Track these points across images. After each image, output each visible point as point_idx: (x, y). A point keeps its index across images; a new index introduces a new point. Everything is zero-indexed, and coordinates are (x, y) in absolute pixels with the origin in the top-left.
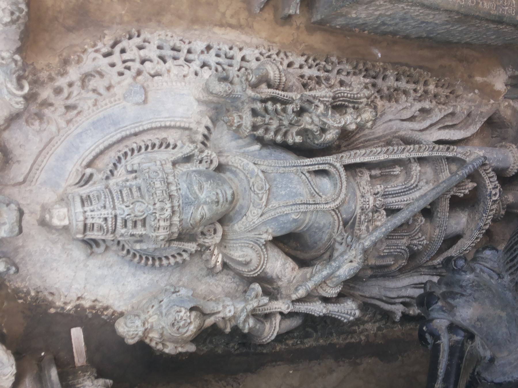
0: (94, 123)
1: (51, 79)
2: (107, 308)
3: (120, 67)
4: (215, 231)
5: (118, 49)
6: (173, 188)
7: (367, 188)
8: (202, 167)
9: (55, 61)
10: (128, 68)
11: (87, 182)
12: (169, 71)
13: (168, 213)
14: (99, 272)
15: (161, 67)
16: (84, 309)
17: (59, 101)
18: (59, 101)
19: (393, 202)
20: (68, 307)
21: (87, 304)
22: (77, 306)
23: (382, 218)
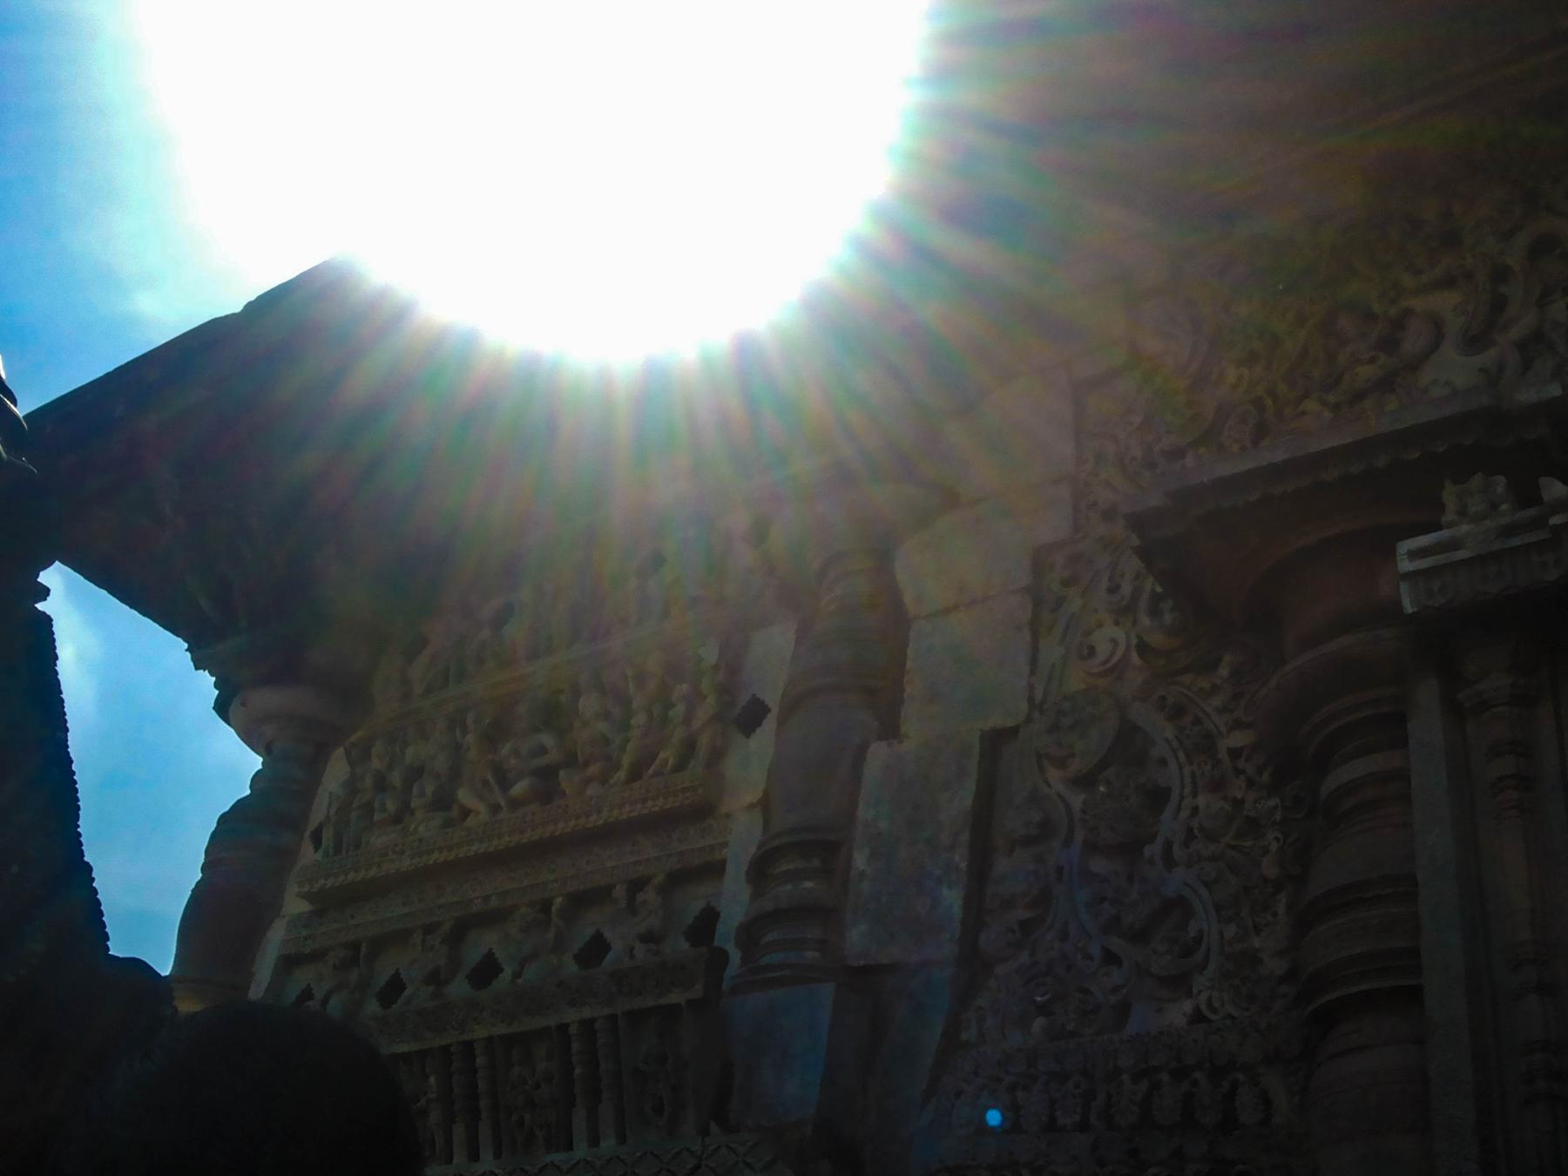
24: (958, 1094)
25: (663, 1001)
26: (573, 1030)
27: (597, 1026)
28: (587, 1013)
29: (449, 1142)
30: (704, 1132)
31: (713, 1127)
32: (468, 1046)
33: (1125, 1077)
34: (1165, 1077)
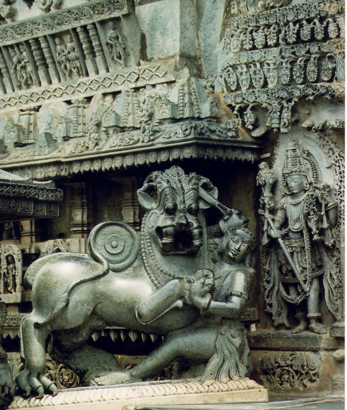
1: (331, 140)
3: (336, 159)
5: (341, 158)
6: (294, 173)
9: (335, 140)
10: (336, 162)
12: (337, 175)
13: (288, 172)
15: (338, 173)
17: (325, 142)
18: (325, 142)
19: (295, 254)
21: (275, 157)
24: (232, 36)
25: (112, 16)
26: (78, 30)
27: (88, 28)
28: (83, 23)
29: (38, 77)
30: (139, 64)
31: (142, 62)
32: (37, 40)
33: (291, 24)
34: (304, 22)
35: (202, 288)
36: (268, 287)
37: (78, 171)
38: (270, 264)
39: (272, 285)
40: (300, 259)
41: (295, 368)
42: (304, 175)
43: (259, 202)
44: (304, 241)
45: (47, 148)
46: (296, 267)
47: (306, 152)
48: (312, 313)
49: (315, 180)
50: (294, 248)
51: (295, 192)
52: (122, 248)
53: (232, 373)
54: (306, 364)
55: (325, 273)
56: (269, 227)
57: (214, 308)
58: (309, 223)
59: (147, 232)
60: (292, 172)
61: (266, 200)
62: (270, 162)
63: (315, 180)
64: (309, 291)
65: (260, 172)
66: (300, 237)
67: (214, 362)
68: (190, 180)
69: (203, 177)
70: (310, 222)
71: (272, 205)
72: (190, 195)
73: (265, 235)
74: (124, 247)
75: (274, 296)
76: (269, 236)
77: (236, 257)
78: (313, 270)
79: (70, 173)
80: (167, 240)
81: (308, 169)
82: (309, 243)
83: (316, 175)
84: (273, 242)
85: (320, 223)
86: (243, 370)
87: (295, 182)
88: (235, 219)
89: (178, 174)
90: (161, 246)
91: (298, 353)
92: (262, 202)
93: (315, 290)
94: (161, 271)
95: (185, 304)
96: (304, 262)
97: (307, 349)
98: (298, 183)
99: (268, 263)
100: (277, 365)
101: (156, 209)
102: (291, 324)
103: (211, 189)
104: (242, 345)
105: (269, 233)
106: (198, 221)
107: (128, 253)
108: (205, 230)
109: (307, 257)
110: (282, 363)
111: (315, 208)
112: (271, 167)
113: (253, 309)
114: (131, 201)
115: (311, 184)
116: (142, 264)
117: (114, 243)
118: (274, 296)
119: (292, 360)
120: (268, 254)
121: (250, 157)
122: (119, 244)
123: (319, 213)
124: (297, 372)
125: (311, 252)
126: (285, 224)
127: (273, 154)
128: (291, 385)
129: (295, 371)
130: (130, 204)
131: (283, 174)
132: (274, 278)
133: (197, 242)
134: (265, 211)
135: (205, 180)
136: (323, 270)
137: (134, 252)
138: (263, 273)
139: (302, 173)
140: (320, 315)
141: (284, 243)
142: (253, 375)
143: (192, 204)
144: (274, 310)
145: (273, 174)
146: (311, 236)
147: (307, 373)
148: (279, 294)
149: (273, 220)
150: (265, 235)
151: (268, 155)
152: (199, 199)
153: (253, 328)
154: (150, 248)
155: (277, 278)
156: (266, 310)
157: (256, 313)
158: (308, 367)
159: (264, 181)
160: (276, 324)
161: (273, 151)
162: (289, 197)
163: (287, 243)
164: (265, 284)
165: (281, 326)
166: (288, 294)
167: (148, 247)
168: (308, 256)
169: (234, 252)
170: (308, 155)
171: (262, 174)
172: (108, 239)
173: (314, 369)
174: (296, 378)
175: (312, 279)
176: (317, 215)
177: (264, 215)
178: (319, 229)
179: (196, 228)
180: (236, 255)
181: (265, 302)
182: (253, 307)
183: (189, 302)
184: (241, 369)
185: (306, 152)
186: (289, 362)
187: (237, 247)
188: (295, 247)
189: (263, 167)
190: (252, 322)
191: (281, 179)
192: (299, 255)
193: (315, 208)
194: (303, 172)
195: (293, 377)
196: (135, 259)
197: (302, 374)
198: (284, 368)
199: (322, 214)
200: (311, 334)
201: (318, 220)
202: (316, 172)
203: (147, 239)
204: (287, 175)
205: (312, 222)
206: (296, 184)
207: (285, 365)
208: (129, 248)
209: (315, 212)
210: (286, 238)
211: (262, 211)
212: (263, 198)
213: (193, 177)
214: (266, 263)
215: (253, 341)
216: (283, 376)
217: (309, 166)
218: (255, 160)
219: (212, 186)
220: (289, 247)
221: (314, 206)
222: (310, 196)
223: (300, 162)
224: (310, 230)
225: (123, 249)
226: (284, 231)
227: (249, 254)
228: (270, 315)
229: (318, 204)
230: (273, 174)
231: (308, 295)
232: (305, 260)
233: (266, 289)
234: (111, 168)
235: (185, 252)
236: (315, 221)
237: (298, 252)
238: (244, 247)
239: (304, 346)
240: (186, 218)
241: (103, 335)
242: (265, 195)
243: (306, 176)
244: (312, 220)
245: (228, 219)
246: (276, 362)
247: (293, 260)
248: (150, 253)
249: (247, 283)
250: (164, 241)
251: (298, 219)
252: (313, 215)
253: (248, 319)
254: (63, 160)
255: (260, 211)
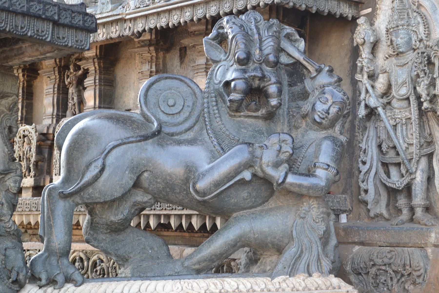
0: (434, 4)
2: (376, 19)
4: (394, 52)
6: (401, 27)
7: (404, 115)
8: (414, 42)
11: (413, 4)
13: (393, 26)
14: (387, 14)
16: (376, 11)
19: (399, 128)
20: (378, 6)
21: (378, 12)
22: (378, 9)
23: (392, 122)
35: (278, 156)
36: (364, 169)
37: (142, 29)
38: (367, 141)
39: (368, 167)
40: (405, 133)
41: (394, 268)
42: (413, 31)
43: (357, 65)
44: (410, 110)
45: (110, 4)
46: (399, 143)
47: (416, 4)
48: (418, 199)
49: (427, 37)
50: (398, 120)
51: (401, 50)
52: (181, 108)
53: (313, 268)
54: (408, 263)
55: (436, 151)
56: (368, 95)
57: (291, 184)
58: (418, 88)
59: (212, 88)
60: (398, 26)
61: (365, 62)
62: (371, 18)
63: (427, 37)
64: (416, 172)
65: (359, 28)
66: (405, 106)
67: (291, 252)
68: (271, 26)
69: (287, 27)
70: (419, 86)
71: (372, 68)
72: (269, 45)
73: (363, 104)
74: (183, 106)
75: (371, 179)
76: (367, 106)
77: (324, 121)
78: (421, 146)
79: (133, 32)
80: (235, 96)
81: (419, 23)
82: (417, 113)
83: (428, 31)
84: (372, 113)
85: (432, 88)
86: (326, 264)
87: (401, 38)
88: (324, 79)
89: (255, 19)
90: (228, 104)
91: (399, 249)
92: (359, 64)
93: (423, 171)
94: (228, 136)
95: (254, 175)
96: (410, 136)
97: (410, 245)
98: (405, 39)
99: (365, 139)
100: (372, 263)
101: (225, 60)
102: (390, 215)
103: (296, 41)
104: (327, 233)
105: (367, 102)
106: (278, 76)
107: (188, 114)
108: (286, 89)
109: (414, 130)
110: (379, 261)
111: (426, 68)
112: (372, 24)
113: (344, 196)
114: (205, 66)
115: (421, 40)
116: (204, 126)
117: (171, 102)
118: (371, 179)
119: (390, 259)
120: (365, 128)
121: (346, 10)
122: (178, 103)
123: (430, 75)
124: (396, 272)
125: (419, 124)
126: (387, 93)
127: (375, 10)
128: (388, 289)
129: (393, 271)
130: (203, 70)
131: (387, 28)
132: (372, 158)
133: (274, 102)
134: (363, 76)
135: (289, 29)
136: (433, 147)
137: (196, 113)
138: (357, 152)
139: (410, 28)
140: (428, 202)
141: (385, 114)
142: (339, 272)
143: (270, 54)
144: (370, 197)
145: (374, 31)
146: (420, 104)
147: (409, 275)
148: (377, 176)
149: (373, 87)
150: (363, 104)
151: (370, 10)
152: (280, 50)
153: (344, 219)
154: (215, 108)
155: (375, 158)
156: (360, 197)
157: (348, 200)
158: (411, 267)
159: (363, 39)
160: (372, 214)
161: (375, 6)
162: (393, 58)
163: (389, 114)
164: (361, 165)
165: (379, 216)
166: (389, 177)
167: (213, 107)
168: (414, 128)
169: (321, 115)
170: (418, 8)
171: (361, 30)
172: (164, 96)
173: (419, 270)
174: (395, 280)
175: (420, 158)
176: (429, 77)
177: (361, 81)
178: (431, 95)
179: (275, 83)
180: (323, 119)
181: (359, 187)
182: (344, 194)
183: (260, 174)
184: (323, 263)
185: (416, 4)
186: (386, 260)
187: (325, 107)
188: (399, 118)
189: (362, 22)
190: (344, 212)
191: (384, 38)
192: (404, 128)
193: (426, 68)
194: (412, 26)
195: (391, 278)
196: (197, 122)
197: (403, 275)
198: (381, 267)
199: (435, 76)
200: (416, 226)
201: (430, 83)
202: (428, 27)
203: (212, 97)
204: (392, 30)
205: (422, 86)
206: (403, 41)
207: (381, 264)
208: (190, 109)
209: (425, 74)
210: (388, 107)
211: (360, 76)
212: (361, 60)
213: (273, 24)
214: (362, 140)
215: (342, 233)
216: (379, 277)
217: (419, 19)
218: (353, 17)
219: (298, 37)
220: (392, 119)
221: (425, 66)
222: (420, 54)
223: (408, 15)
224: (418, 97)
225: (183, 108)
226: (385, 100)
227: (341, 119)
228: (366, 203)
229: (430, 63)
230: (374, 31)
231: (413, 176)
232: (412, 135)
233: (361, 172)
234: (180, 23)
235: (259, 113)
236: (427, 85)
237: (402, 124)
238: (334, 110)
239: (407, 240)
240: (261, 69)
241: (162, 222)
242: (364, 56)
243: (416, 32)
244: (422, 83)
245: (315, 77)
246: (371, 260)
247: (396, 134)
248: (215, 114)
249: (337, 153)
250: (231, 98)
251: (404, 83)
252: (423, 77)
253: (337, 207)
254: (128, 17)
255: (358, 77)
